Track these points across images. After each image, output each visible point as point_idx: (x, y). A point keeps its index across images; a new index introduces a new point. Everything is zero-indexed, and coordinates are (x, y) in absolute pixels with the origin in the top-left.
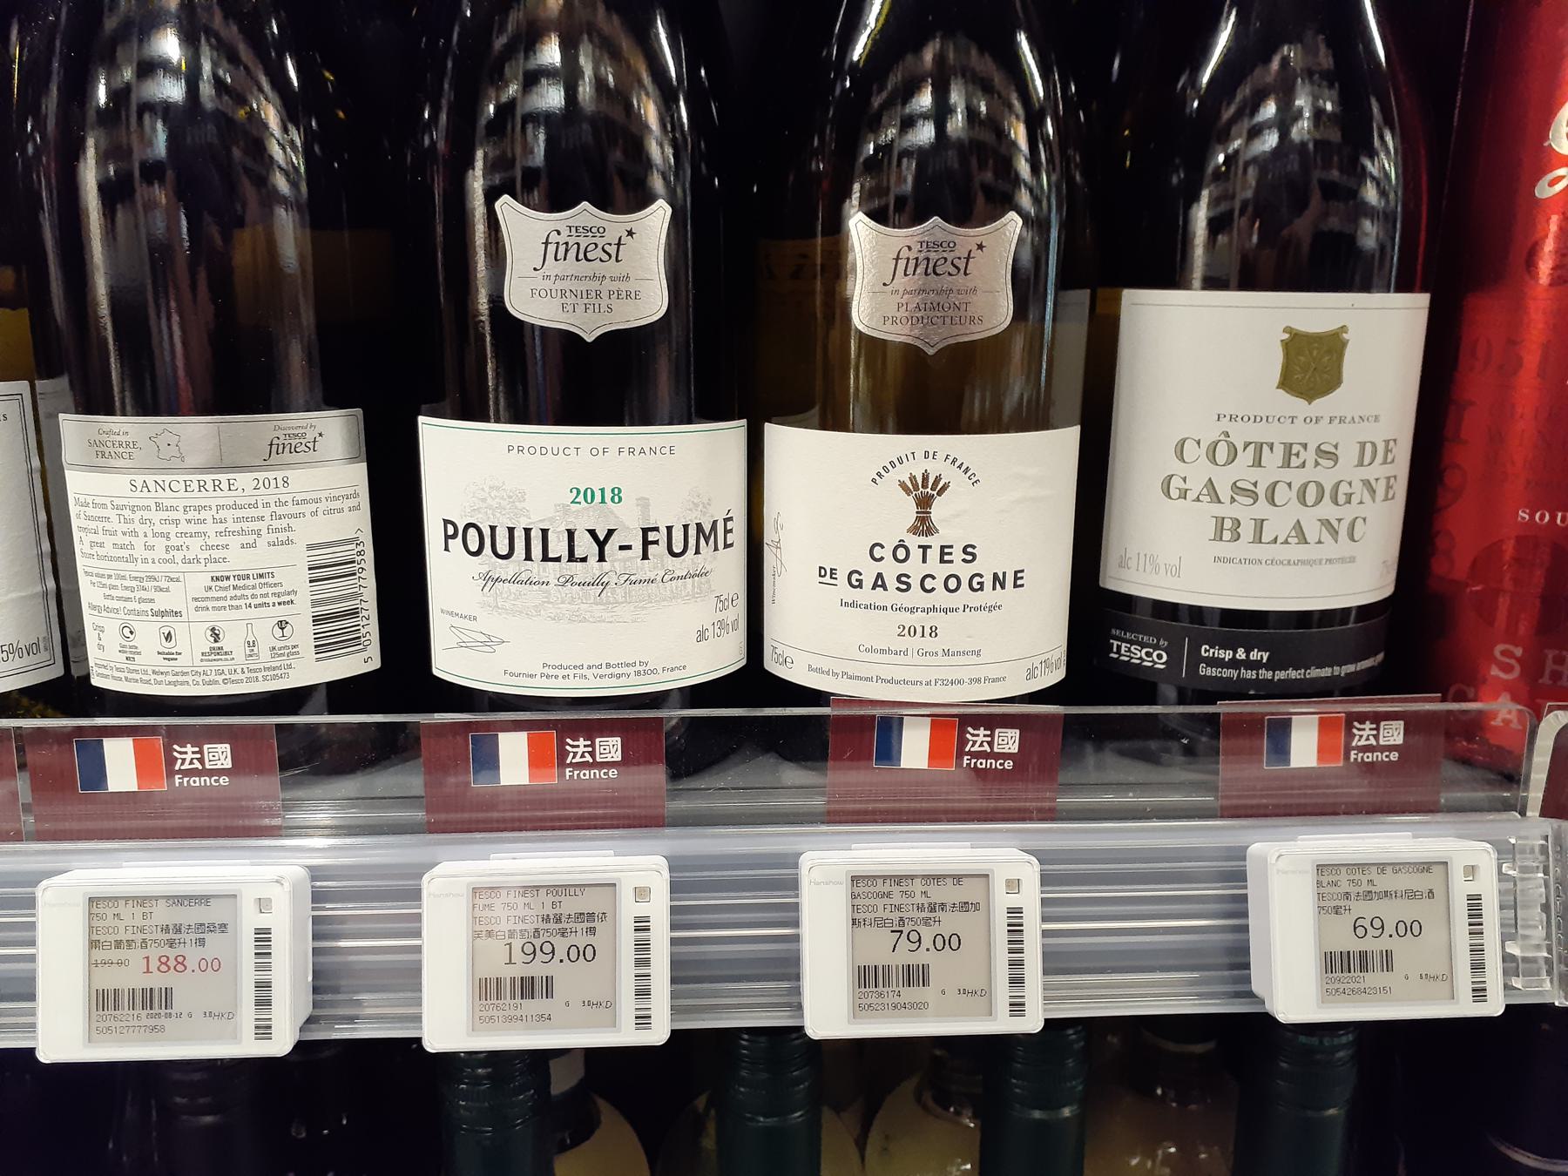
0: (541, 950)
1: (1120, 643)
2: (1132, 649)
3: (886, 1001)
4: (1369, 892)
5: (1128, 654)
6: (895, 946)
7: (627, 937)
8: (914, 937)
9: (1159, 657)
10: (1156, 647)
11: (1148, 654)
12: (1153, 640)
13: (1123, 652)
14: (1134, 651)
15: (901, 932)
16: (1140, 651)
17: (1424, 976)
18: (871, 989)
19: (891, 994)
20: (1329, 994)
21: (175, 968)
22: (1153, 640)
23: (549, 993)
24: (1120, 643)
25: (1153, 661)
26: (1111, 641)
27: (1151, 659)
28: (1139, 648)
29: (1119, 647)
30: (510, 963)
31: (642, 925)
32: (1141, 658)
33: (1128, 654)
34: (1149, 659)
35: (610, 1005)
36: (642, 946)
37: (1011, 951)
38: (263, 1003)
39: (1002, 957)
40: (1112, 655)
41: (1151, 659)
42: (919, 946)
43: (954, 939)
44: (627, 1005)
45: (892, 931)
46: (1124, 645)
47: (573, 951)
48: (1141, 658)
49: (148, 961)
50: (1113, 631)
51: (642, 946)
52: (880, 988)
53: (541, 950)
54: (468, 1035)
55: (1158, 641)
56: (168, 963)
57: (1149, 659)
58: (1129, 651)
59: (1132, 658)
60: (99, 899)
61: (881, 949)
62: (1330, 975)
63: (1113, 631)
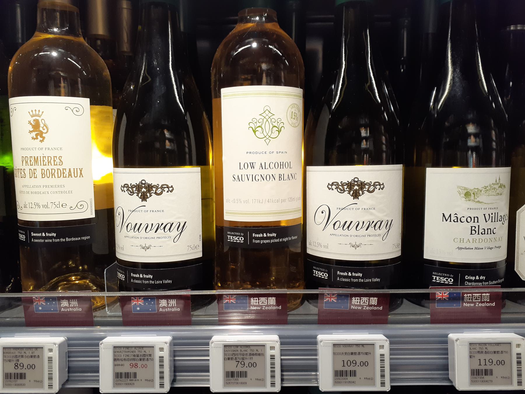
0: (353, 363)
1: (436, 277)
2: (441, 278)
3: (231, 381)
4: (144, 355)
5: (439, 280)
6: (237, 366)
7: (268, 361)
8: (243, 363)
9: (451, 280)
10: (449, 277)
11: (447, 280)
12: (448, 275)
13: (437, 280)
14: (442, 279)
15: (239, 362)
16: (444, 279)
17: (502, 377)
18: (345, 377)
19: (232, 380)
20: (473, 382)
21: (135, 367)
22: (448, 275)
23: (246, 376)
24: (436, 277)
25: (448, 282)
26: (433, 276)
27: (448, 281)
28: (443, 278)
29: (436, 278)
30: (480, 365)
31: (273, 357)
32: (444, 281)
33: (439, 280)
34: (447, 281)
35: (152, 381)
36: (273, 364)
37: (271, 368)
38: (162, 378)
39: (268, 369)
40: (433, 281)
41: (448, 281)
42: (244, 366)
43: (366, 363)
44: (269, 380)
45: (236, 361)
46: (438, 277)
47: (250, 364)
48: (444, 281)
49: (480, 360)
50: (433, 273)
51: (273, 364)
52: (235, 378)
53: (353, 363)
54: (223, 388)
55: (450, 275)
56: (137, 365)
57: (447, 281)
58: (440, 279)
59: (441, 281)
60: (473, 344)
61: (233, 366)
62: (473, 376)
63: (433, 273)
